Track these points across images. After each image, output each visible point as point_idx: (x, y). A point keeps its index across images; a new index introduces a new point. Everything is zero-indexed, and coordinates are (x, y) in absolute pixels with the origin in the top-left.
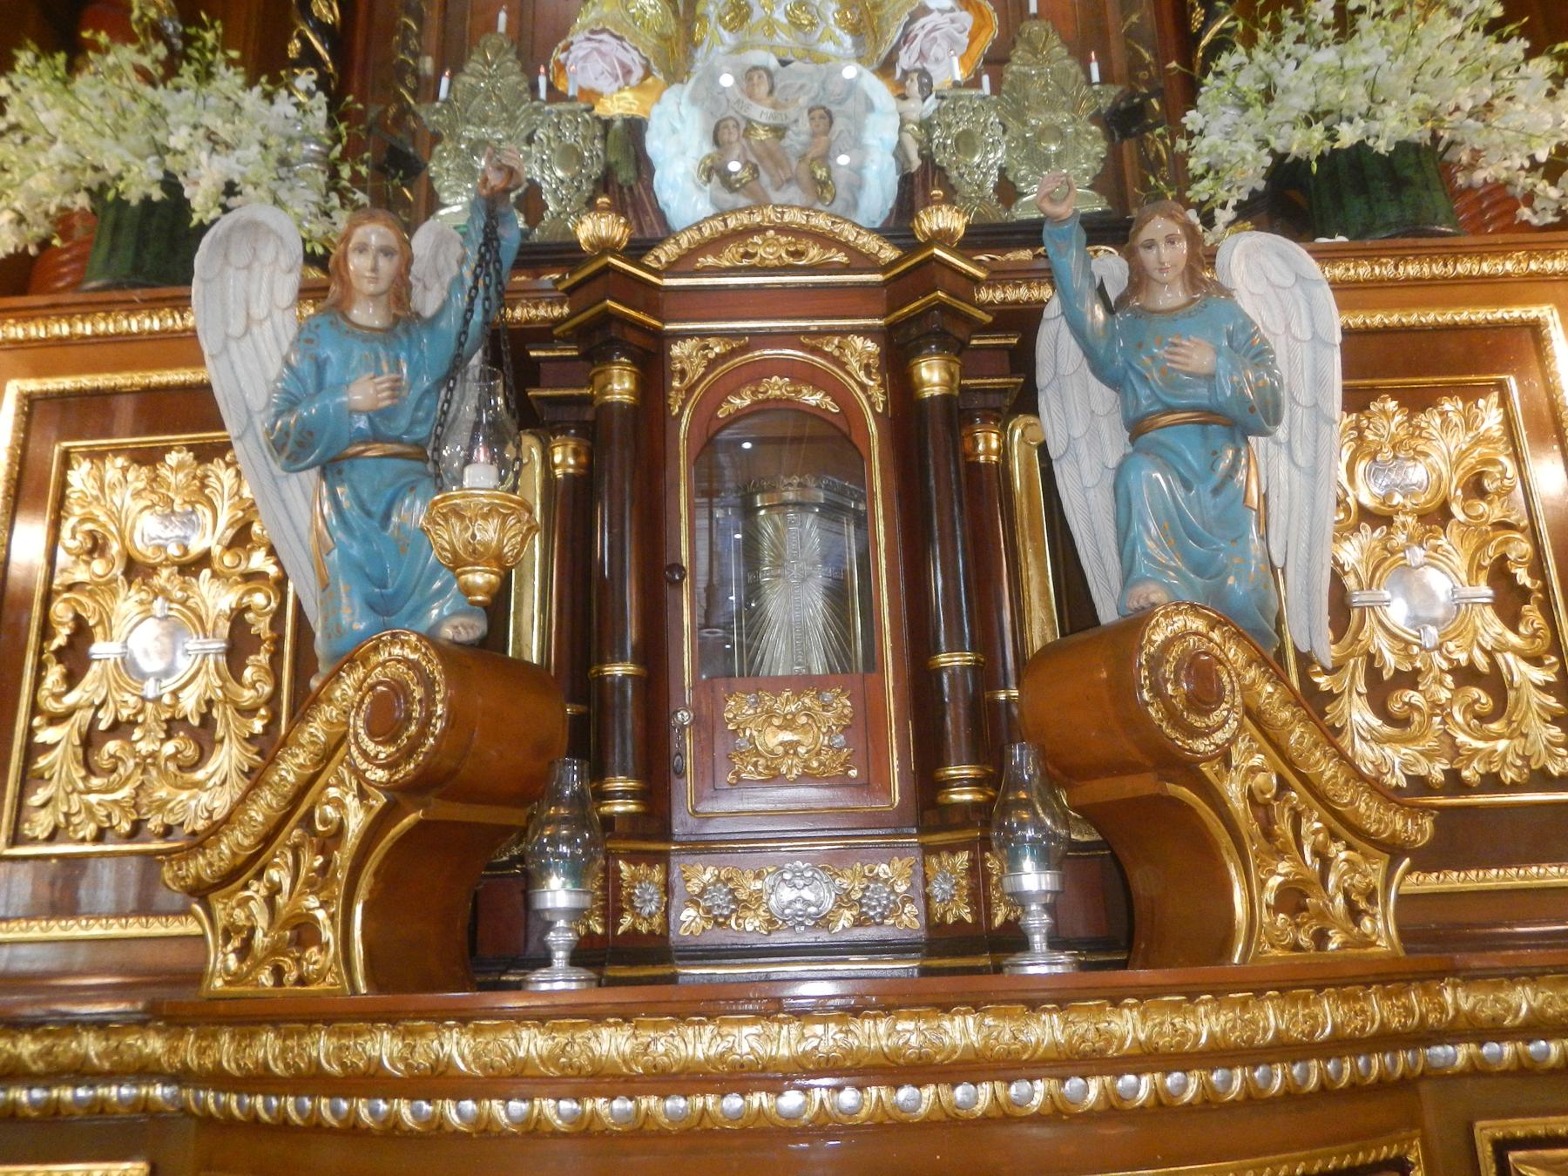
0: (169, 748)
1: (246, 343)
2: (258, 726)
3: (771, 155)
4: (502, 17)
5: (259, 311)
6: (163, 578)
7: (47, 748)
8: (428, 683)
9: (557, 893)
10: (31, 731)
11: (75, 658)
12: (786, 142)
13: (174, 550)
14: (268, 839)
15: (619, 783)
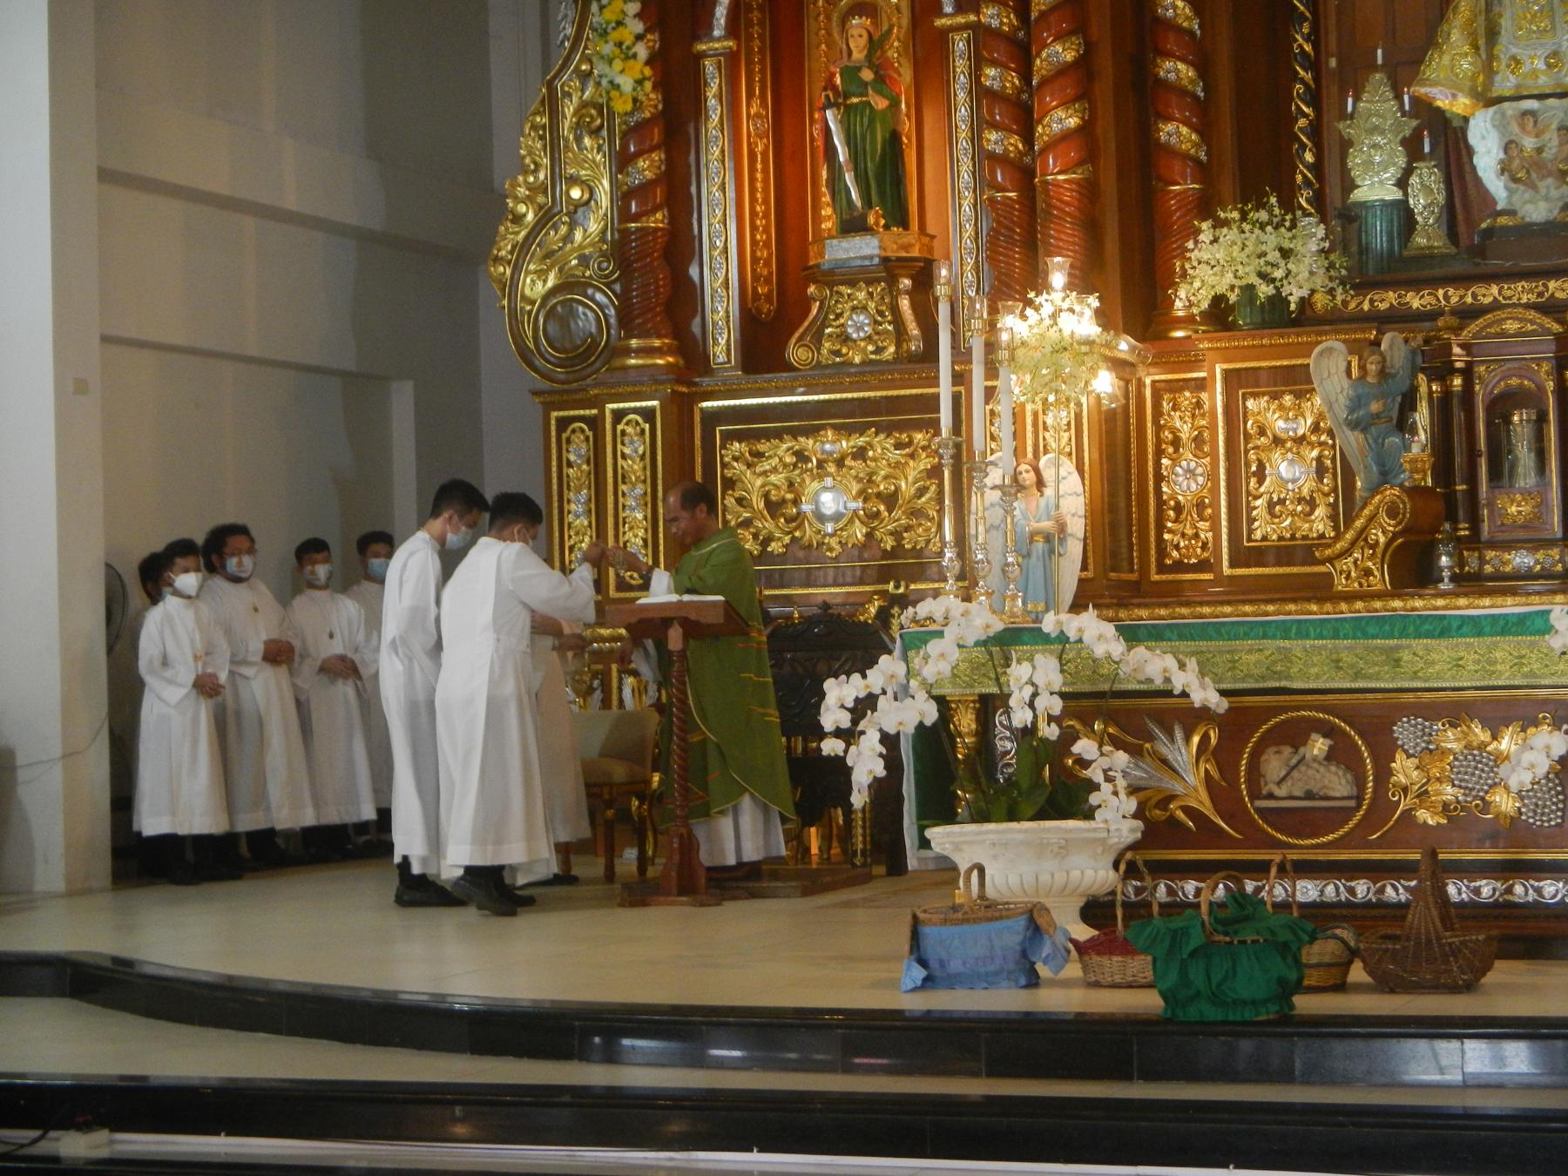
0: (1299, 508)
1: (1328, 381)
2: (1332, 500)
3: (1535, 164)
4: (1379, 52)
5: (1333, 371)
6: (1289, 444)
7: (1255, 508)
8: (1404, 503)
9: (1444, 560)
10: (1248, 502)
11: (1261, 476)
12: (1544, 155)
13: (1291, 433)
14: (1353, 543)
15: (1461, 526)
